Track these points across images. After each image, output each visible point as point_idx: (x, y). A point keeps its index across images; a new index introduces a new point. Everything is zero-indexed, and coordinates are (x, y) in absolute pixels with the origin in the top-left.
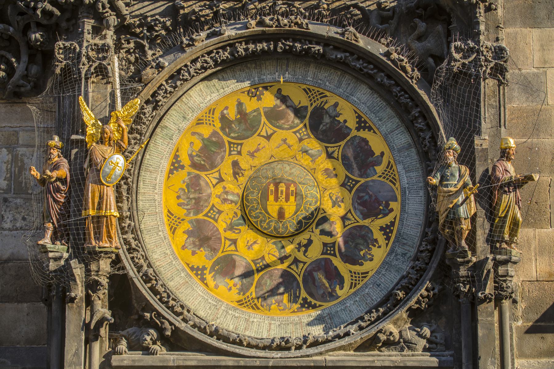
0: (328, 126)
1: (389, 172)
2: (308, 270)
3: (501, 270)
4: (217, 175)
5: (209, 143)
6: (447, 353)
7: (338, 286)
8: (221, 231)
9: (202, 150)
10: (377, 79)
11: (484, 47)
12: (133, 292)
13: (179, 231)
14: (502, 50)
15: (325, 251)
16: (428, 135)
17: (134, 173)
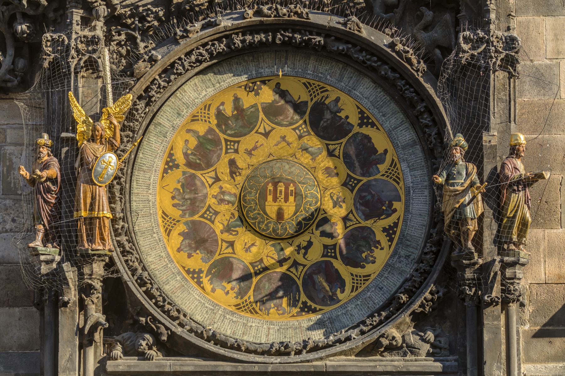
0: (329, 122)
1: (393, 170)
3: (509, 272)
4: (213, 174)
5: (205, 141)
6: (451, 358)
7: (339, 290)
8: (218, 232)
9: (197, 148)
10: (381, 72)
11: (495, 37)
12: (127, 295)
13: (175, 233)
14: (513, 39)
15: (325, 253)
16: (434, 132)
17: (127, 173)
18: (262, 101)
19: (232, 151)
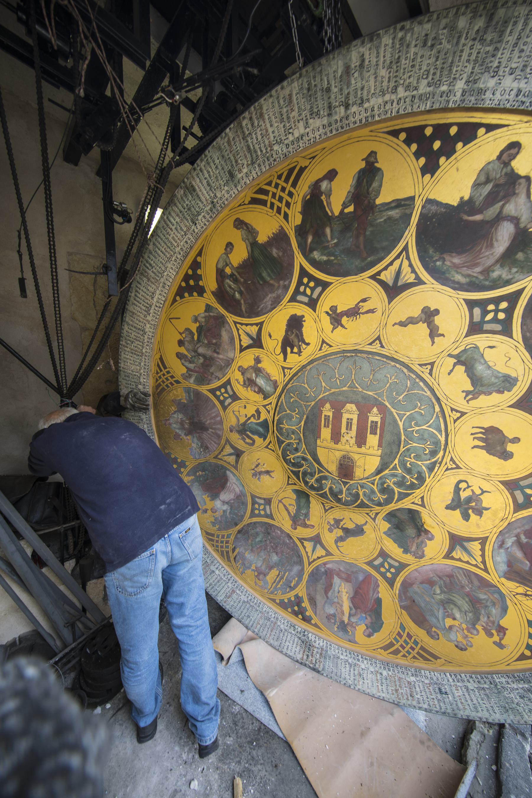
2: (327, 566)
5: (261, 258)
8: (226, 426)
18: (431, 197)
19: (306, 300)
